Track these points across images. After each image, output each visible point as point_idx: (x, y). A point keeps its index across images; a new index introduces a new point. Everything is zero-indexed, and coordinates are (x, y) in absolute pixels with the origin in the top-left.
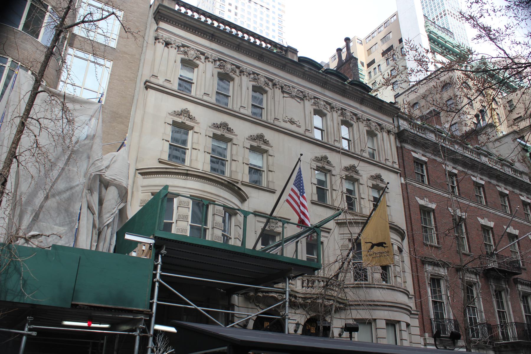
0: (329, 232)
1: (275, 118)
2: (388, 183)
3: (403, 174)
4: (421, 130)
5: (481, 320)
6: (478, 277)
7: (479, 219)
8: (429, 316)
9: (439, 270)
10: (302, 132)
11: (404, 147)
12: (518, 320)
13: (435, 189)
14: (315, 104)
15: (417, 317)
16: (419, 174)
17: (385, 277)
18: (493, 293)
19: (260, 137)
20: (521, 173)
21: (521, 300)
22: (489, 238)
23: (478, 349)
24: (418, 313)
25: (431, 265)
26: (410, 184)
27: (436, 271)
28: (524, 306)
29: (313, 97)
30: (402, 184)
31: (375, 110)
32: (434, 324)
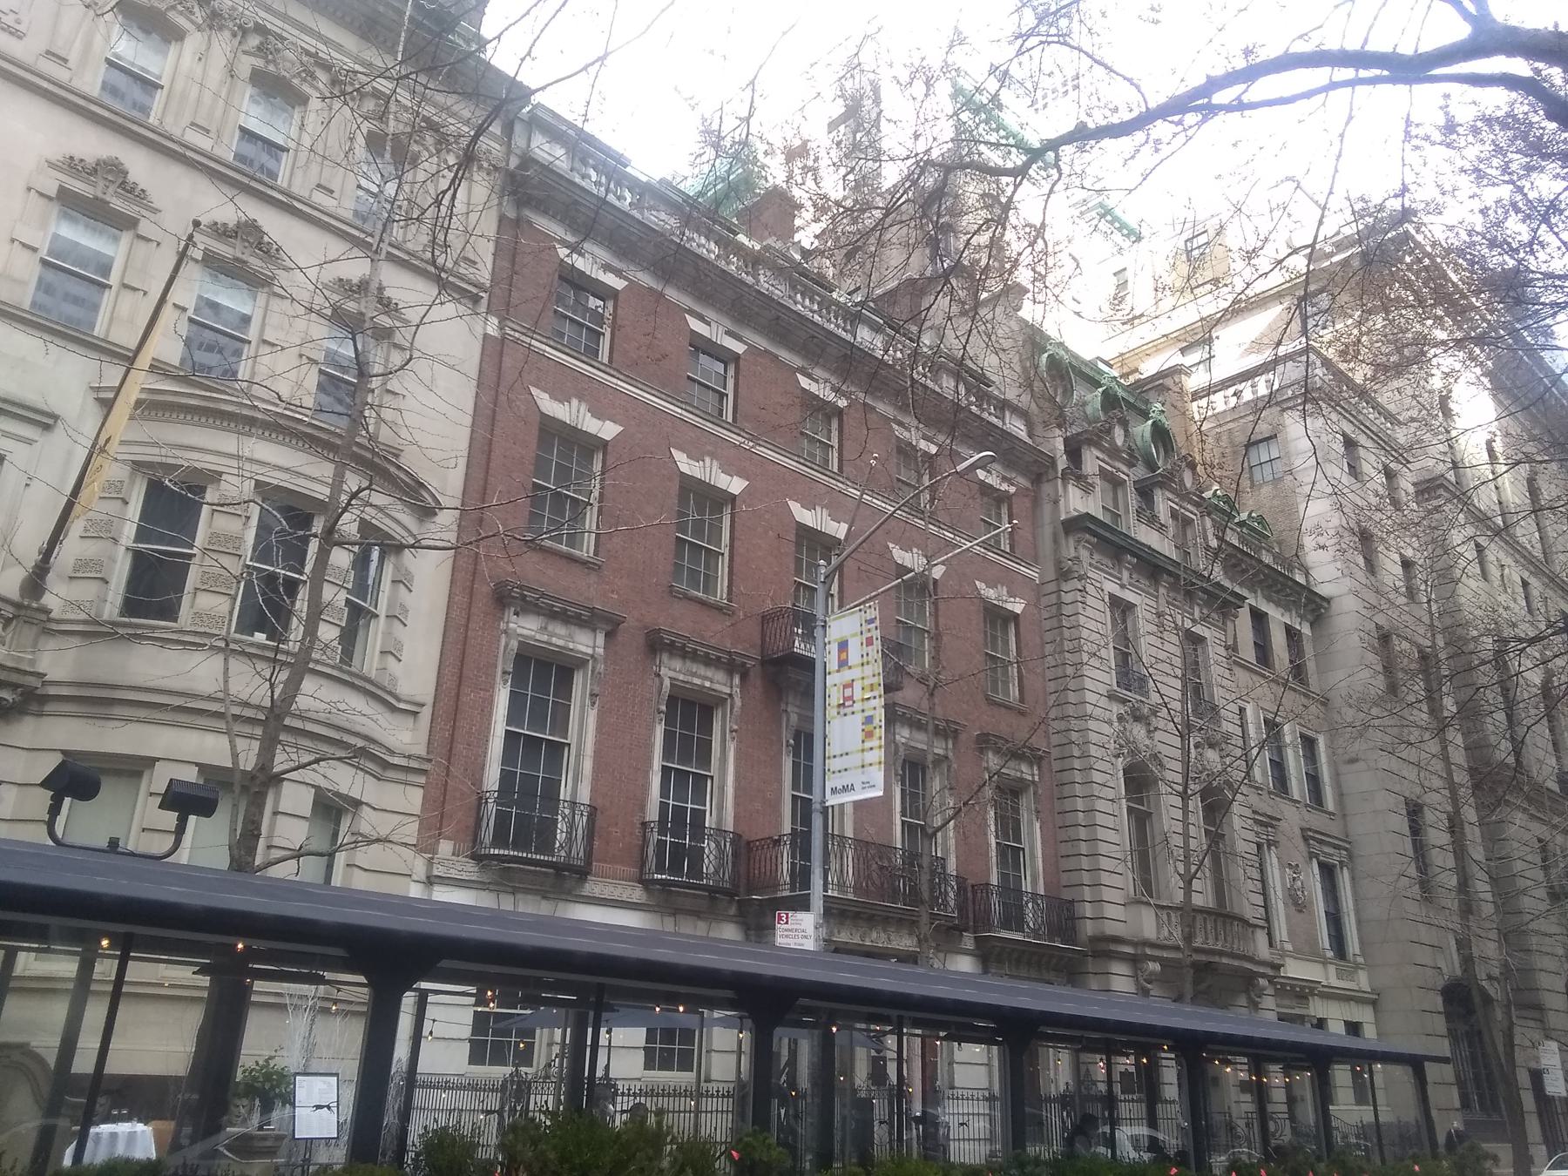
0: (47, 428)
1: (319, 186)
2: (197, 224)
3: (504, 311)
4: (845, 322)
5: (720, 819)
6: (737, 680)
7: (795, 507)
8: (478, 781)
9: (570, 636)
10: (28, 59)
11: (530, 223)
12: (871, 833)
13: (629, 380)
14: (261, 50)
15: (422, 780)
16: (581, 325)
17: (349, 637)
18: (787, 737)
19: (248, 232)
20: (1003, 406)
21: (896, 775)
22: (1006, 642)
23: (674, 915)
24: (426, 766)
25: (539, 614)
26: (516, 341)
27: (552, 635)
28: (796, 765)
29: (251, 25)
30: (486, 336)
32: (492, 807)
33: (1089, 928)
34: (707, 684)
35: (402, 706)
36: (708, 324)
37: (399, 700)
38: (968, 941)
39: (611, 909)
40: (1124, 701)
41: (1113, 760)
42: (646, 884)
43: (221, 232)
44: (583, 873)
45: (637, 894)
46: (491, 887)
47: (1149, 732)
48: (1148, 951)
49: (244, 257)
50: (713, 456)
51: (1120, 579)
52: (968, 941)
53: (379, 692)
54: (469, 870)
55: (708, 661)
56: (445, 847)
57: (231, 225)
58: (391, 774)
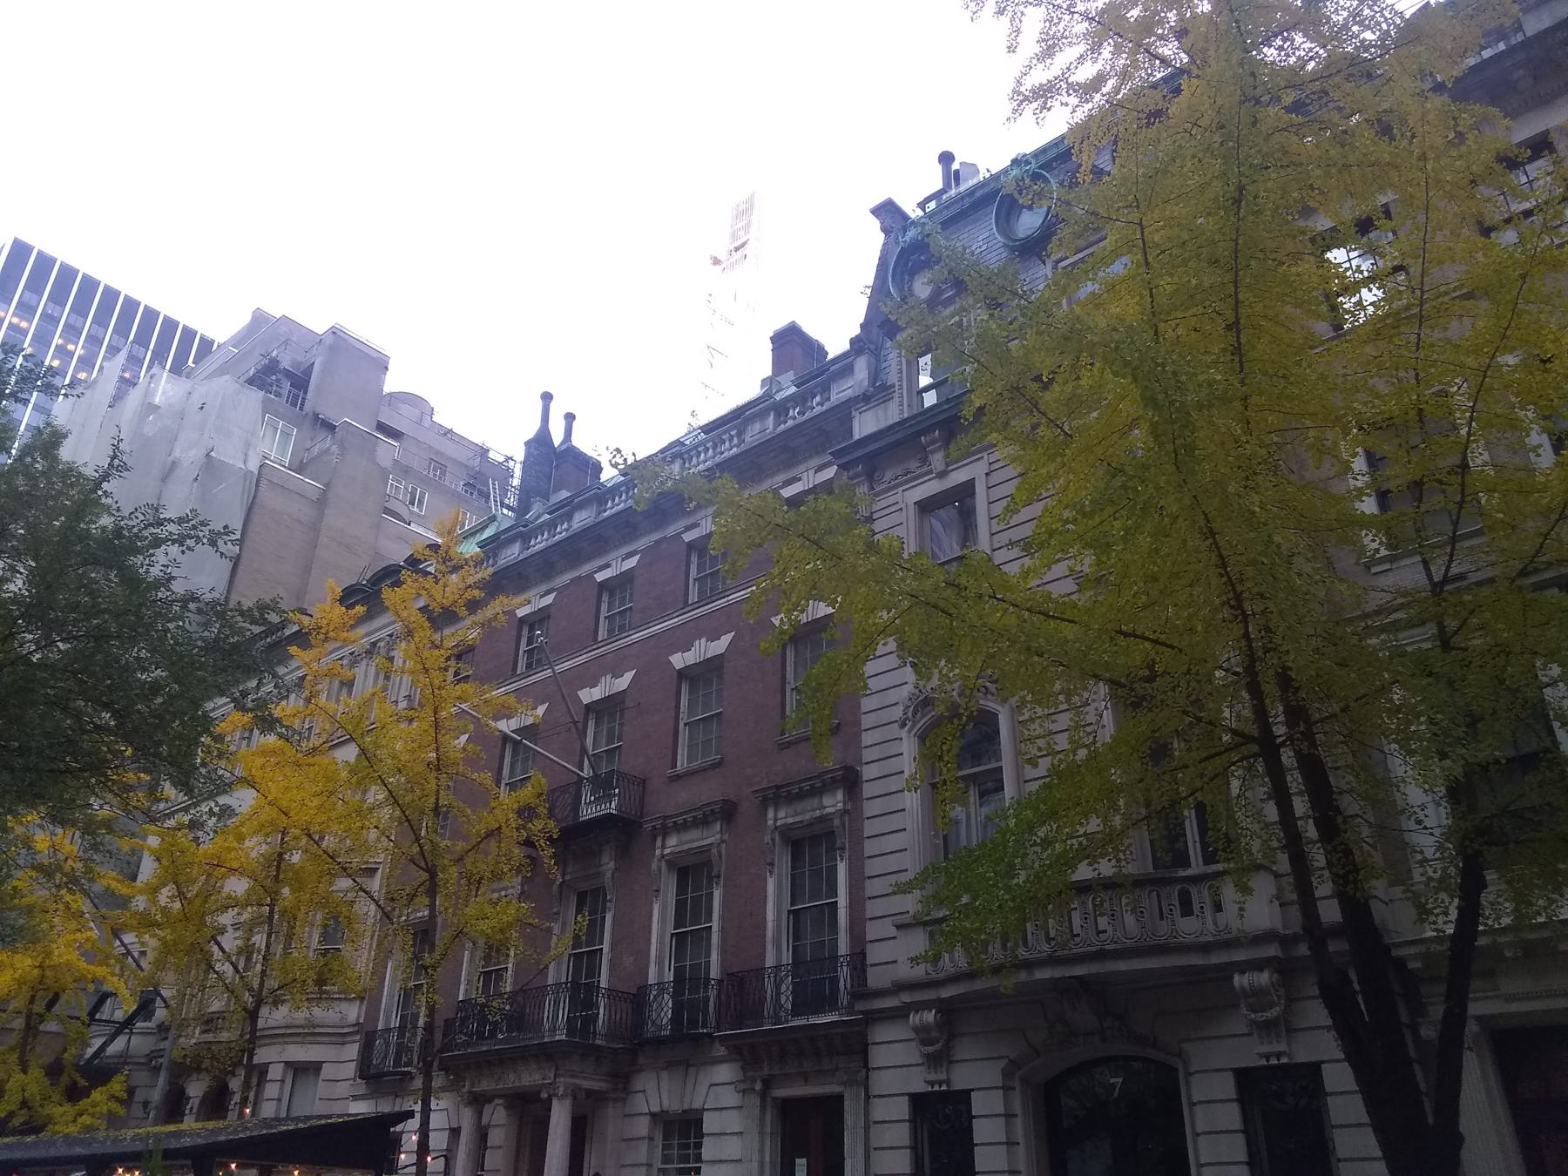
15: (358, 1037)
48: (906, 997)
51: (931, 472)
58: (348, 1039)
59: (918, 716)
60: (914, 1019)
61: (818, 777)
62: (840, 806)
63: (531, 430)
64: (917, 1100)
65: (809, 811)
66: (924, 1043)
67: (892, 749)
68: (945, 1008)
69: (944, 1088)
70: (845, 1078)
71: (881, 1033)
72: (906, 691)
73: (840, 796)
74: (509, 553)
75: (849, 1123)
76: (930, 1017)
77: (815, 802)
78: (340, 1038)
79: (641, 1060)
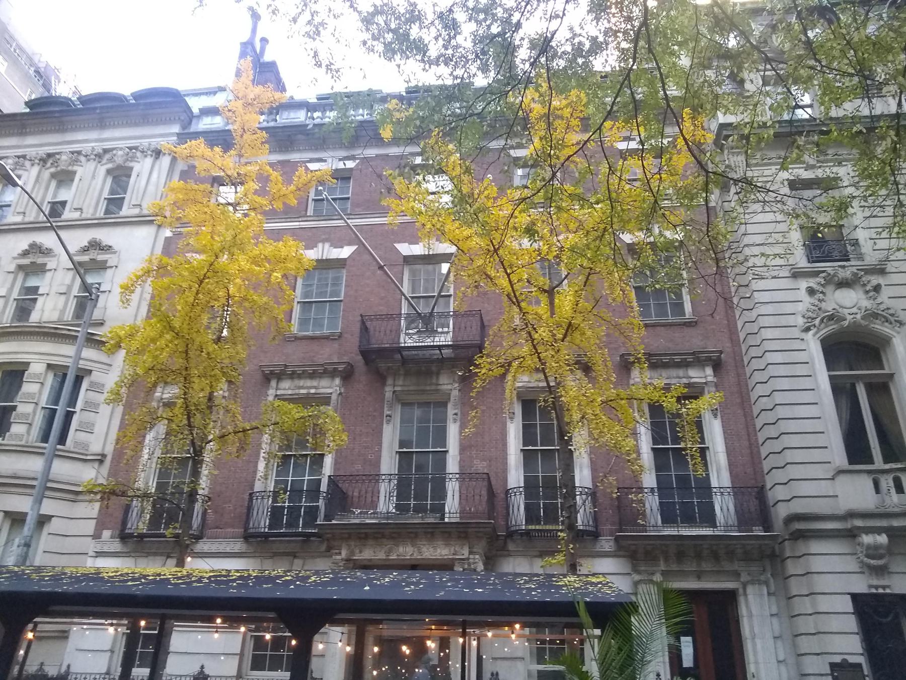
6: (337, 381)
12: (480, 466)
31: (136, 125)
33: (782, 512)
34: (313, 391)
35: (89, 458)
36: (325, 161)
37: (87, 455)
38: (606, 544)
39: (221, 559)
40: (816, 274)
41: (803, 335)
42: (248, 537)
43: (25, 254)
44: (198, 538)
45: (238, 546)
46: (132, 554)
47: (867, 292)
48: (859, 523)
49: (34, 260)
50: (324, 241)
52: (606, 544)
53: (71, 455)
54: (117, 546)
55: (313, 375)
56: (106, 534)
57: (27, 247)
58: (80, 497)
59: (823, 325)
60: (867, 539)
61: (693, 354)
62: (710, 379)
63: (246, 38)
64: (855, 597)
65: (674, 377)
66: (868, 556)
67: (797, 345)
68: (891, 532)
69: (888, 591)
70: (749, 578)
71: (816, 546)
72: (801, 308)
73: (709, 371)
74: (292, 115)
75: (754, 612)
76: (883, 539)
77: (681, 372)
78: (74, 494)
79: (511, 546)
